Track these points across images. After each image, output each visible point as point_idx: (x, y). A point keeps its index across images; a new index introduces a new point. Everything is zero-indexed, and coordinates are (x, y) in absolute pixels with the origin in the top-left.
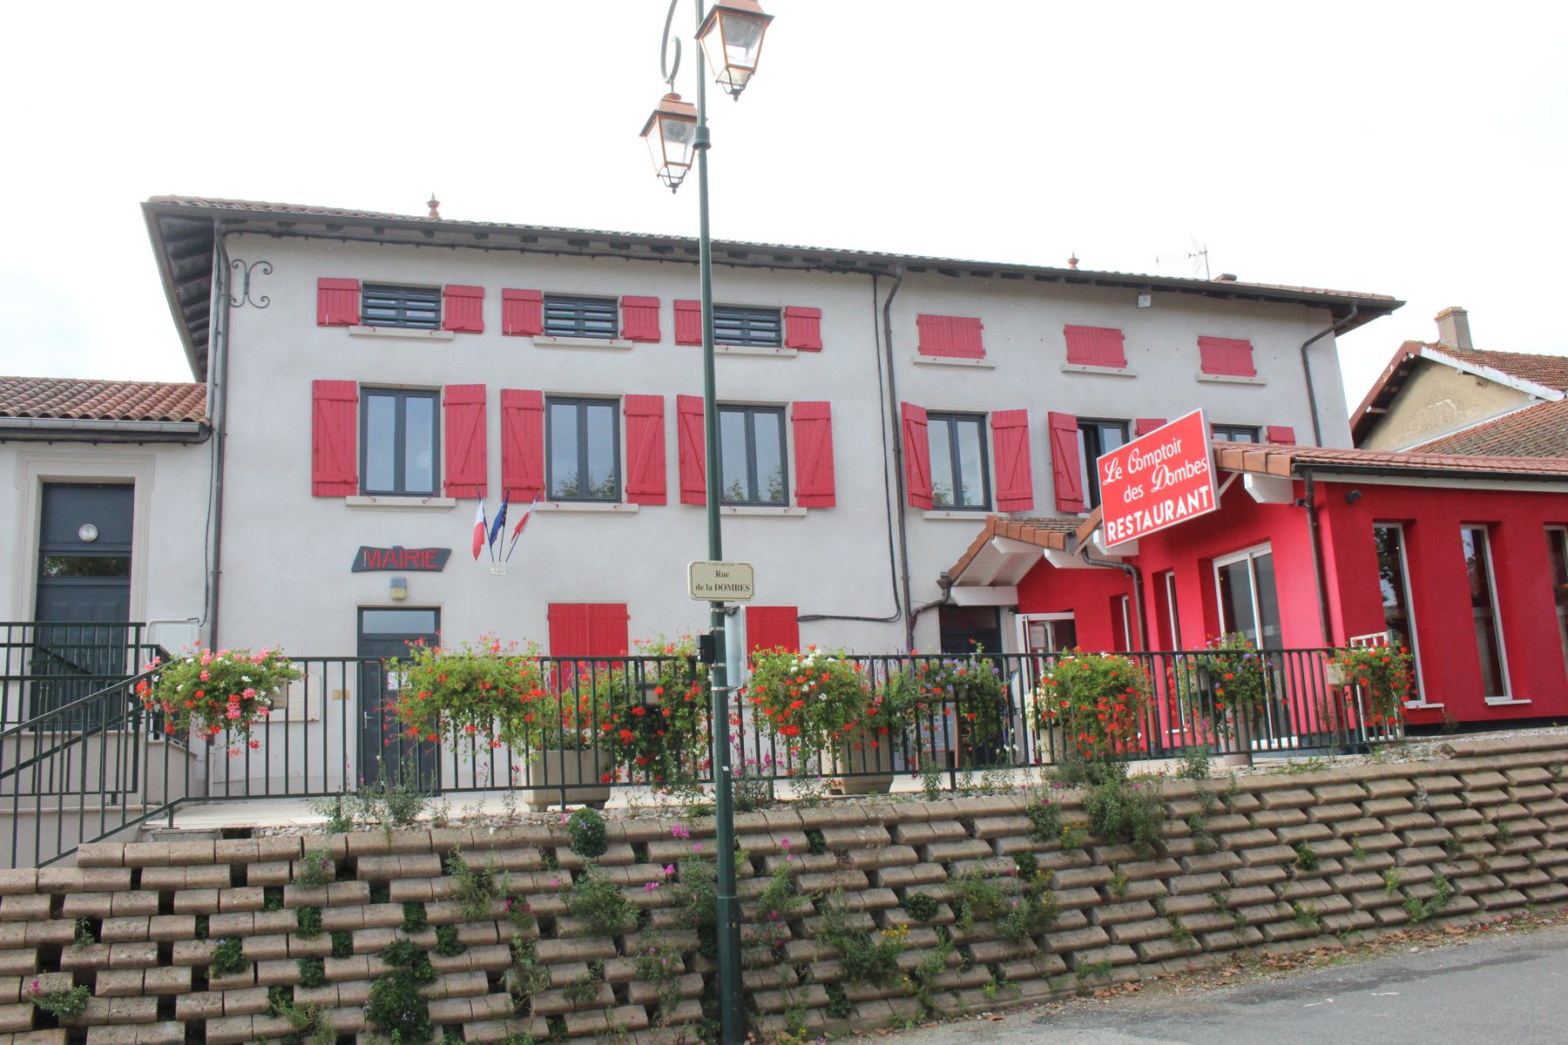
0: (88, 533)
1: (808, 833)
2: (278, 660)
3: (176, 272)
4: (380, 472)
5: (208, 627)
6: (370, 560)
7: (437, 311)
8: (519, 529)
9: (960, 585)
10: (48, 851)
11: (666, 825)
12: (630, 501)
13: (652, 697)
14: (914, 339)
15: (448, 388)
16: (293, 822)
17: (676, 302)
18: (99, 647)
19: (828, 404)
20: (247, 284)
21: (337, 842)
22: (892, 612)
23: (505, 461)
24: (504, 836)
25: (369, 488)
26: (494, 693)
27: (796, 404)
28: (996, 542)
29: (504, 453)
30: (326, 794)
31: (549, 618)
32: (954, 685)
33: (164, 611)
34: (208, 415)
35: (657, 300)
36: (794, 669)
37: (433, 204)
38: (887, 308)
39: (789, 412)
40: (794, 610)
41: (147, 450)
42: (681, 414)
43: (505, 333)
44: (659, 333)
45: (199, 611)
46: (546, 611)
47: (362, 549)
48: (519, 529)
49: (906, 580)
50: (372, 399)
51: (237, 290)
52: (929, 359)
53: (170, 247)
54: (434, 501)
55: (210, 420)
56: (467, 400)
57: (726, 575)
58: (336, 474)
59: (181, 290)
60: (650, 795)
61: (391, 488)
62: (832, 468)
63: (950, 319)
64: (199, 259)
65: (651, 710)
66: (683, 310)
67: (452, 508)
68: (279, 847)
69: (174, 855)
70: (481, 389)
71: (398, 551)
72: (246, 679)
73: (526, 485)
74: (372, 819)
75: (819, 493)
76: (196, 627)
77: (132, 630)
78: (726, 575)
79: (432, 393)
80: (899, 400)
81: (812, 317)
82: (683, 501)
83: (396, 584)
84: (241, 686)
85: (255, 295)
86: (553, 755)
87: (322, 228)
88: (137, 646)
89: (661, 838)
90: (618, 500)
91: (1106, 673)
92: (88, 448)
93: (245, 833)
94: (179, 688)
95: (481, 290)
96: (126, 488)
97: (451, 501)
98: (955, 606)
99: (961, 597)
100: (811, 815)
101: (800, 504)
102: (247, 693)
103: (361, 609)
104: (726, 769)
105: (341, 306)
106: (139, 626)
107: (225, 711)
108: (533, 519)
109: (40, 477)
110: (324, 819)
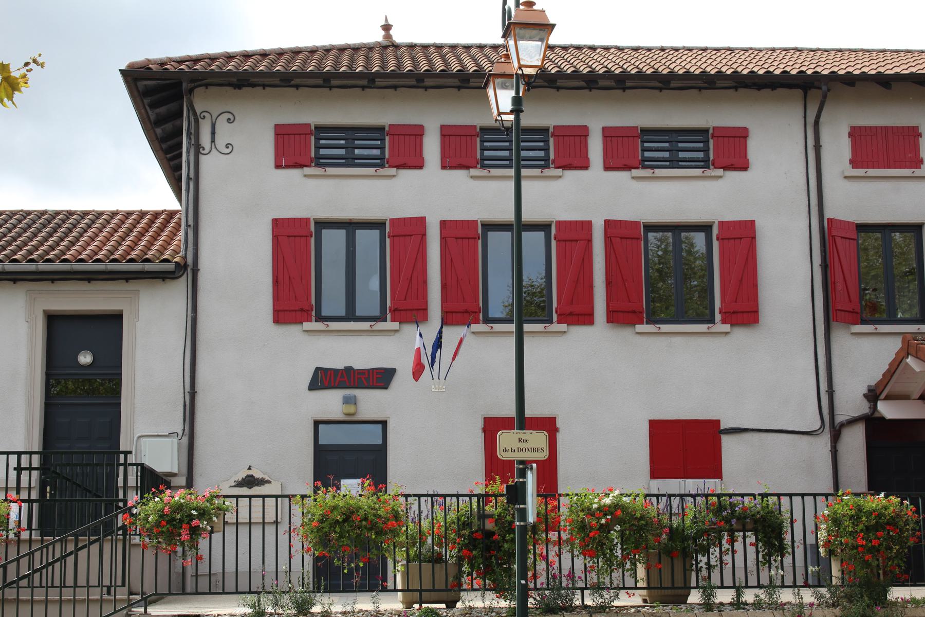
0: (85, 358)
2: (218, 497)
3: (152, 118)
4: (334, 302)
5: (185, 440)
6: (324, 379)
7: (382, 148)
9: (887, 398)
12: (559, 322)
13: (489, 525)
14: (847, 154)
17: (604, 129)
18: (97, 465)
19: (753, 223)
20: (213, 133)
22: (817, 425)
25: (324, 313)
26: (364, 523)
27: (721, 224)
28: (910, 360)
29: (442, 281)
30: (250, 592)
32: (738, 519)
33: (147, 433)
34: (182, 253)
35: (586, 128)
36: (595, 506)
37: (387, 28)
38: (817, 123)
39: (715, 231)
40: (718, 422)
41: (133, 285)
42: (608, 238)
43: (444, 167)
44: (587, 160)
45: (178, 426)
46: (480, 424)
47: (317, 369)
49: (831, 393)
50: (325, 233)
51: (205, 140)
52: (860, 172)
53: (146, 101)
54: (381, 326)
55: (185, 258)
56: (408, 232)
57: (526, 441)
58: (294, 301)
59: (159, 131)
60: (479, 598)
61: (342, 313)
62: (755, 286)
63: (886, 129)
64: (172, 106)
65: (492, 533)
66: (609, 134)
71: (349, 370)
72: (194, 512)
73: (464, 308)
74: (280, 611)
75: (744, 311)
76: (175, 441)
77: (122, 456)
78: (526, 441)
79: (378, 225)
80: (828, 214)
81: (740, 136)
82: (610, 320)
83: (347, 401)
84: (191, 517)
85: (221, 142)
86: (415, 565)
87: (276, 81)
88: (126, 465)
90: (550, 321)
91: (870, 513)
92: (84, 286)
94: (150, 519)
95: (422, 127)
96: (117, 318)
97: (396, 325)
98: (882, 419)
99: (888, 410)
101: (724, 322)
102: (195, 522)
103: (317, 423)
104: (523, 582)
105: (296, 149)
106: (127, 453)
107: (180, 535)
108: (470, 340)
109: (44, 311)
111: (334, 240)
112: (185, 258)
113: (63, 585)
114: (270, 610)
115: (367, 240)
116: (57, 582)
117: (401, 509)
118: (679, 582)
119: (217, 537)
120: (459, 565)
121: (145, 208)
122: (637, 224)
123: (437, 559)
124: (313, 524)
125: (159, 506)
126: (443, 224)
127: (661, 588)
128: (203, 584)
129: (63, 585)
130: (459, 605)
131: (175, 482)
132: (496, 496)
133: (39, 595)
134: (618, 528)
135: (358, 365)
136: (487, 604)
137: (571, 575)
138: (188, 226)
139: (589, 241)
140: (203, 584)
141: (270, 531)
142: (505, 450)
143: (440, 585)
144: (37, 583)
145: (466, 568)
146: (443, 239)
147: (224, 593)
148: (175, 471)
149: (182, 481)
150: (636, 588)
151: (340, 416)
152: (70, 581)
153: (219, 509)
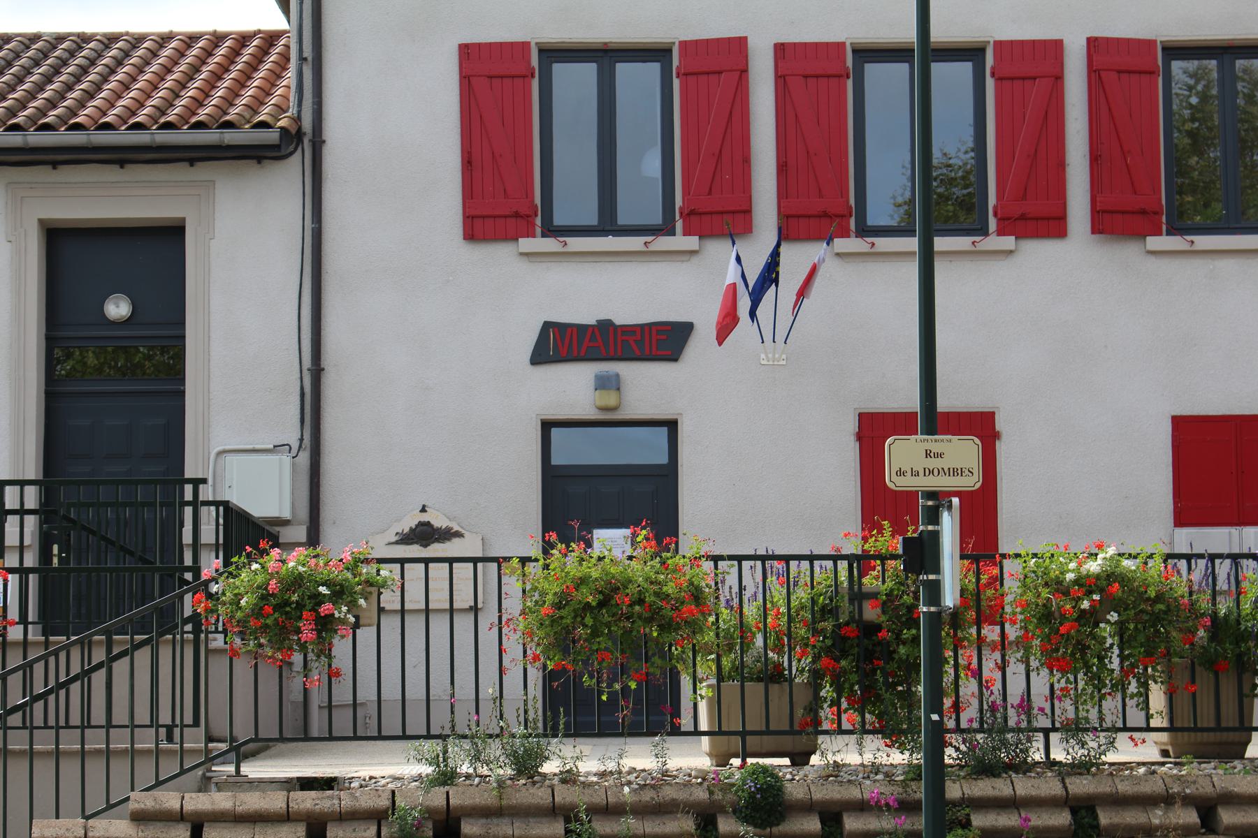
0: (118, 308)
1: (1074, 812)
2: (367, 561)
4: (575, 195)
5: (304, 458)
6: (560, 344)
8: (802, 293)
10: (96, 801)
11: (870, 789)
12: (1001, 232)
13: (871, 613)
15: (684, 45)
16: (388, 770)
18: (143, 504)
21: (437, 798)
23: (782, 168)
24: (647, 796)
25: (559, 220)
26: (637, 608)
30: (429, 736)
31: (860, 437)
33: (235, 446)
34: (292, 111)
36: (1070, 576)
41: (203, 172)
45: (291, 434)
46: (852, 425)
47: (547, 326)
48: (802, 293)
50: (558, 69)
54: (664, 243)
55: (298, 119)
57: (940, 455)
58: (502, 199)
60: (853, 746)
61: (592, 219)
65: (877, 628)
67: (693, 253)
68: (366, 801)
69: (239, 809)
70: (738, 46)
71: (606, 327)
72: (323, 590)
73: (822, 208)
74: (484, 771)
76: (286, 459)
77: (188, 489)
78: (940, 455)
83: (603, 383)
84: (318, 599)
86: (732, 686)
88: (196, 504)
89: (861, 807)
90: (984, 232)
92: (111, 174)
93: (328, 783)
94: (243, 602)
96: (173, 233)
97: (692, 242)
100: (1081, 786)
102: (325, 608)
103: (547, 426)
104: (935, 717)
106: (197, 482)
107: (298, 631)
108: (831, 272)
109: (41, 221)
110: (427, 770)
111: (575, 82)
112: (298, 119)
113: (86, 725)
114: (465, 768)
115: (637, 81)
116: (75, 719)
117: (706, 583)
118: (1230, 716)
119: (366, 635)
120: (815, 685)
121: (222, 28)
122: (1150, 44)
123: (773, 676)
124: (542, 611)
125: (260, 579)
126: (781, 50)
127: (1196, 729)
128: (343, 722)
129: (86, 725)
130: (815, 759)
131: (287, 534)
132: (884, 559)
133: (44, 742)
134: (1113, 617)
135: (625, 315)
136: (868, 758)
137: (1026, 705)
138: (302, 59)
139: (1058, 78)
140: (343, 722)
141: (464, 624)
142: (901, 473)
143: (780, 721)
144: (38, 720)
145: (827, 691)
146: (781, 79)
147: (380, 737)
148: (286, 514)
149: (300, 533)
150: (1149, 729)
151: (591, 414)
152: (98, 716)
153: (369, 583)
